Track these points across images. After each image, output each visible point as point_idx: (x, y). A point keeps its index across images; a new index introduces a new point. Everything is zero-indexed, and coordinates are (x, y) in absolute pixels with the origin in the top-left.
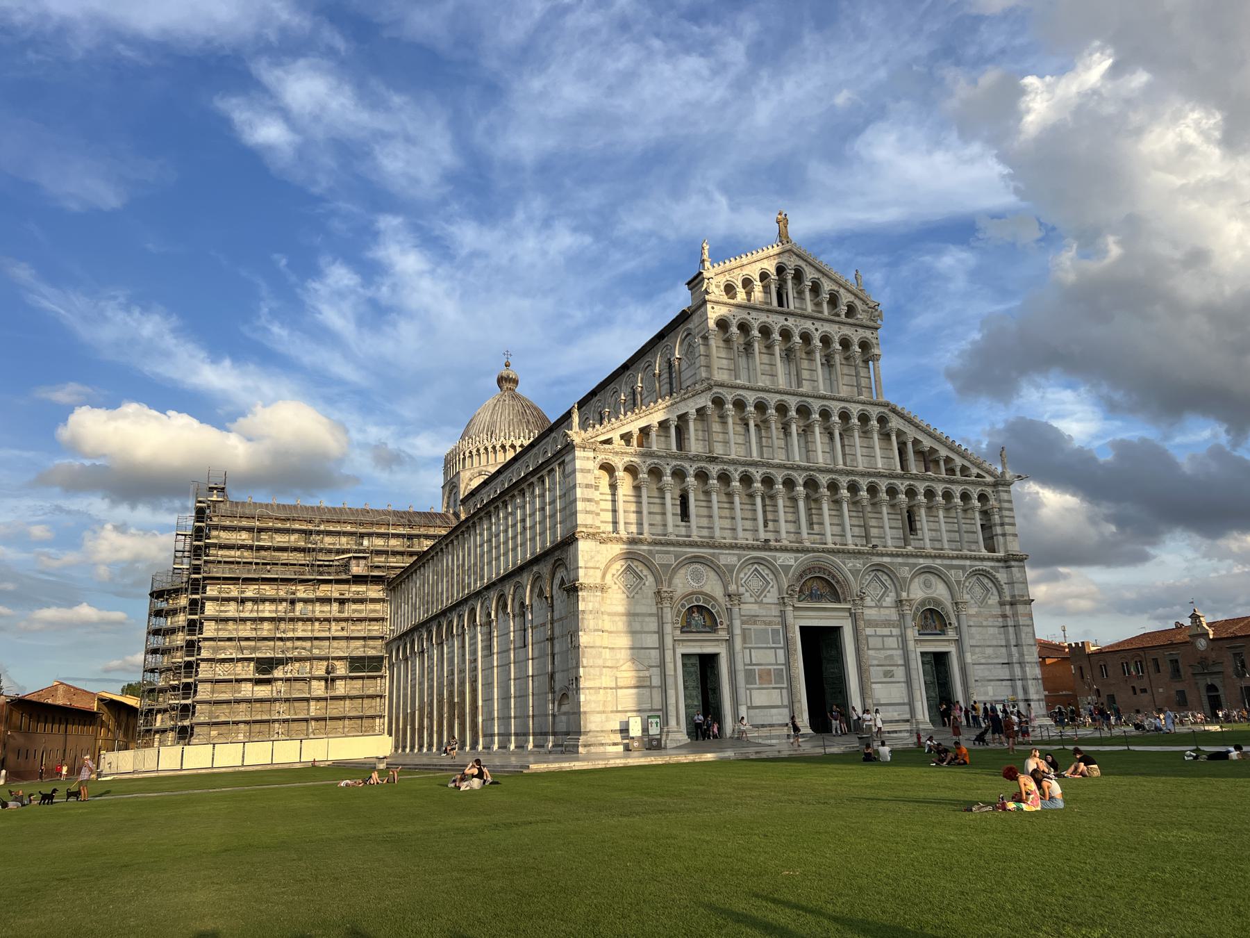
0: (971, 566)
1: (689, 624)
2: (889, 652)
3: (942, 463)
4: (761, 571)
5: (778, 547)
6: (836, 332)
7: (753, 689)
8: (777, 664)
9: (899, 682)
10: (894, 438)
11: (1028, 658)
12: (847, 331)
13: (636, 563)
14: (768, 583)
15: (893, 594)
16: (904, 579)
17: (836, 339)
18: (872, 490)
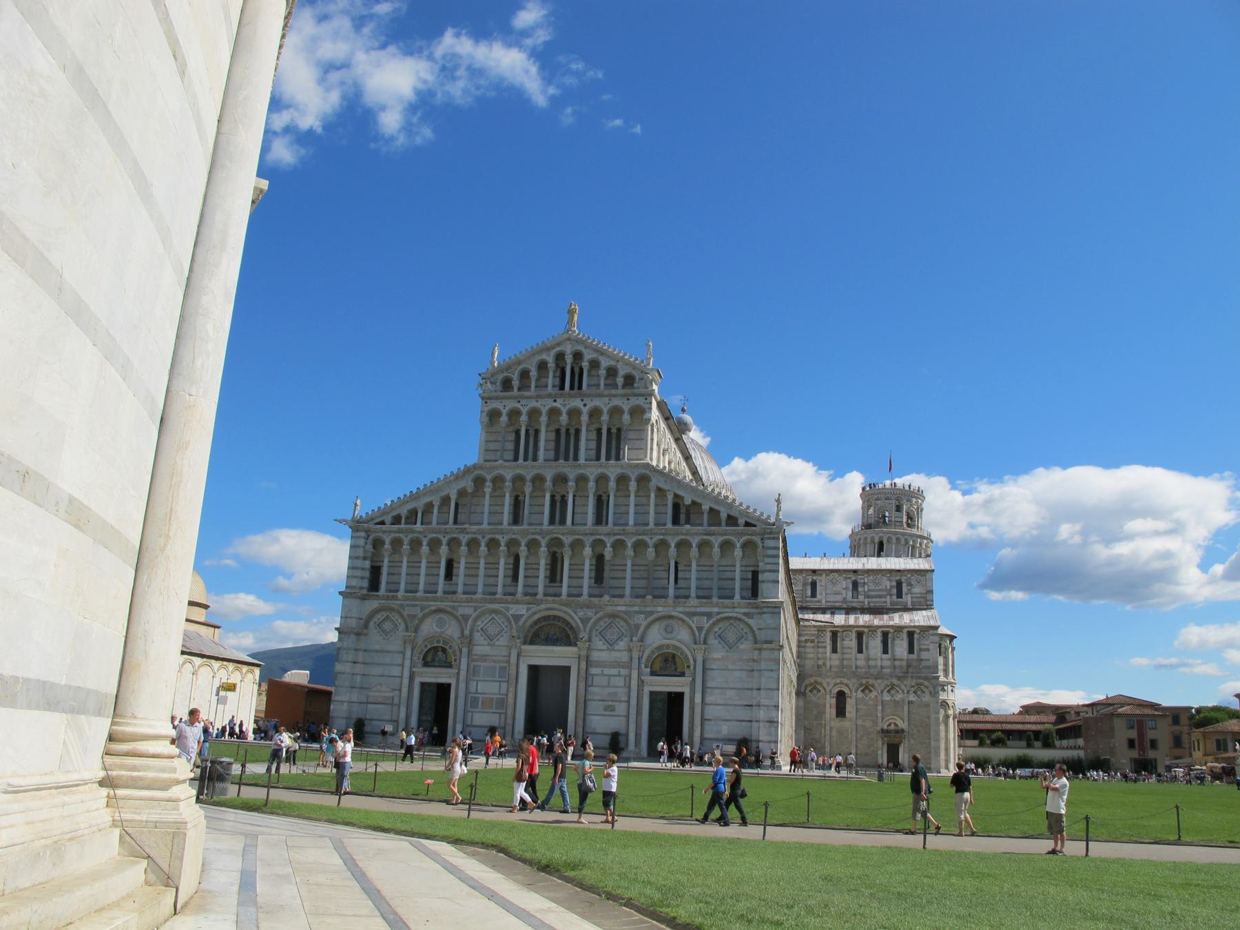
0: (718, 613)
1: (433, 660)
2: (613, 690)
3: (706, 516)
4: (498, 620)
5: (509, 600)
6: (604, 404)
7: (475, 712)
8: (500, 694)
9: (619, 716)
10: (653, 495)
11: (764, 702)
12: (616, 402)
13: (393, 614)
14: (503, 630)
15: (626, 639)
16: (637, 627)
17: (605, 410)
18: (619, 545)
